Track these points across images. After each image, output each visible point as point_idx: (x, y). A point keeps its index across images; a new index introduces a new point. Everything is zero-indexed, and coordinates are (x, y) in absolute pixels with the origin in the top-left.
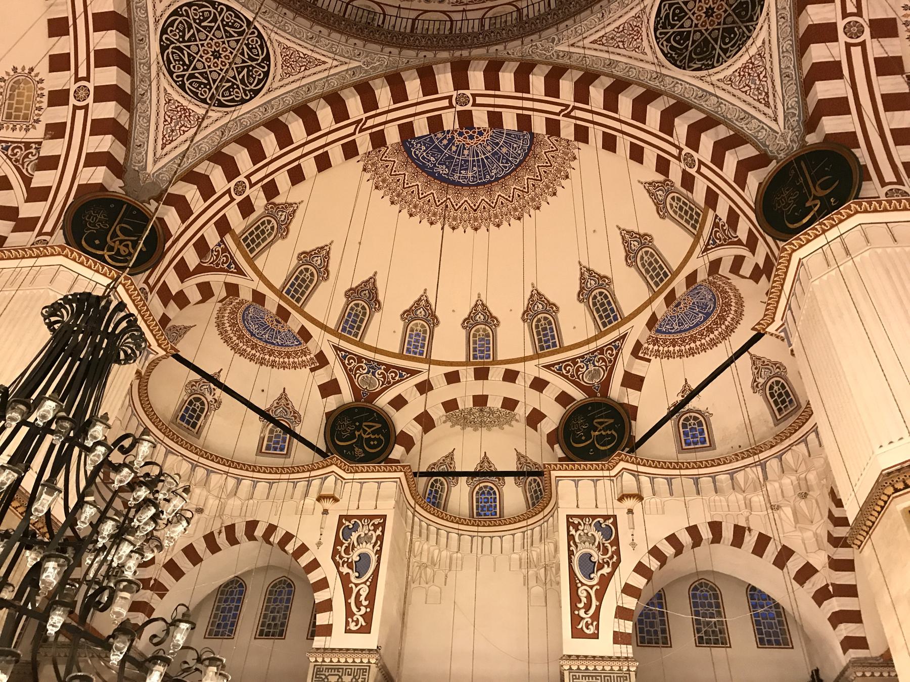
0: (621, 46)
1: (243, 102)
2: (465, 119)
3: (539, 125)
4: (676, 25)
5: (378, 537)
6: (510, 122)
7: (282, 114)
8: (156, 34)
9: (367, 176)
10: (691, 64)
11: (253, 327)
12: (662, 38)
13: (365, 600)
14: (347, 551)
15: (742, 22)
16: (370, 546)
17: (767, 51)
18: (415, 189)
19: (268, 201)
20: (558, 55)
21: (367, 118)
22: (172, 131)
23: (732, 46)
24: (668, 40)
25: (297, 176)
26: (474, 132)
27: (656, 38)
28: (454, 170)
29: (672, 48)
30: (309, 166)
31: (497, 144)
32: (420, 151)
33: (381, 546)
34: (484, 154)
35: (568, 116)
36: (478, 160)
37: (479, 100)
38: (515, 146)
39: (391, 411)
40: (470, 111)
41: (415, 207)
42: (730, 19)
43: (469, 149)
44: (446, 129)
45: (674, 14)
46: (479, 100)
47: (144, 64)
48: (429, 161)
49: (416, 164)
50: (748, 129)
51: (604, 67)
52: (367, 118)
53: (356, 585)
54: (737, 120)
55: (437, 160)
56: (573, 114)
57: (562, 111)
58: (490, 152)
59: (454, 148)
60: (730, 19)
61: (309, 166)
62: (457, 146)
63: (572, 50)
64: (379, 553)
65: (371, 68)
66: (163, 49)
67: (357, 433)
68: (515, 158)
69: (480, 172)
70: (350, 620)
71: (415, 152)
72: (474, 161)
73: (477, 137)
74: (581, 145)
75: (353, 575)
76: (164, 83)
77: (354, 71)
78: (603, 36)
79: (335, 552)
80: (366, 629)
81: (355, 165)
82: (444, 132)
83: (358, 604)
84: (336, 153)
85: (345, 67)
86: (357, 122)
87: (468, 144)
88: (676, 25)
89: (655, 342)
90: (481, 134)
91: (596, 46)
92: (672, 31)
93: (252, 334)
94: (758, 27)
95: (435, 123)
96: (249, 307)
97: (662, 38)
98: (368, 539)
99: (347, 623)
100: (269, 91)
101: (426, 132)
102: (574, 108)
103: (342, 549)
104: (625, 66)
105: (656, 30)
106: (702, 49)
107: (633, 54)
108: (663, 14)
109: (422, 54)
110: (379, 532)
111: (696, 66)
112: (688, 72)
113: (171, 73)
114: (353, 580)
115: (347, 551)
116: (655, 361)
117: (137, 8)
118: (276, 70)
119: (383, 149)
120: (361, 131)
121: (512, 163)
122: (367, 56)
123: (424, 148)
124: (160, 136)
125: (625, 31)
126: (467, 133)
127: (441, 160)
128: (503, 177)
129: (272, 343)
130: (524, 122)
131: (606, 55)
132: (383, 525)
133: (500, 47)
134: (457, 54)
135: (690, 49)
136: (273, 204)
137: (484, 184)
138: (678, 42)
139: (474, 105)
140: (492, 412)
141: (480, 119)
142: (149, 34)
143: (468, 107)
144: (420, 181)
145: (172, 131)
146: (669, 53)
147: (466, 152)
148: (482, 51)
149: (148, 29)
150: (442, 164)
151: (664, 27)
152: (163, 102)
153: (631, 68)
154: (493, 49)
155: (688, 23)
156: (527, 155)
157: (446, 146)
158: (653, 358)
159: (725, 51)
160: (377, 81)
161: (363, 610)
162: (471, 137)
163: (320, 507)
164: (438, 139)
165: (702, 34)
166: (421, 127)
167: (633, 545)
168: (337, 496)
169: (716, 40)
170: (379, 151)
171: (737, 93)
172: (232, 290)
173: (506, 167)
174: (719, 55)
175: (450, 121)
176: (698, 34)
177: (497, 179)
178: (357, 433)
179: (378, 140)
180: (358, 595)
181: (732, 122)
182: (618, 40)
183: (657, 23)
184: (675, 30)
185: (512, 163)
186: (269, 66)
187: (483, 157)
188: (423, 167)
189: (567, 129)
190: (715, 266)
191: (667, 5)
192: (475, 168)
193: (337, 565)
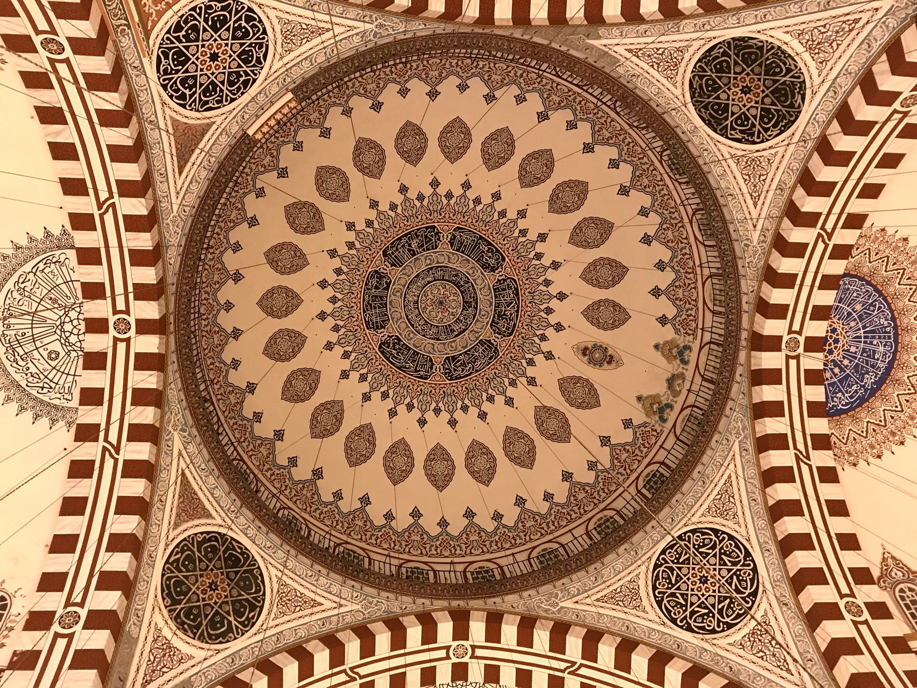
0: (764, 177)
1: (755, 569)
2: (814, 344)
3: (836, 267)
4: (753, 123)
6: (827, 298)
7: (775, 535)
8: (675, 630)
9: (862, 463)
10: (796, 105)
12: (763, 136)
15: (762, 56)
17: (797, 27)
19: (873, 583)
20: (763, 242)
22: (774, 655)
23: (785, 64)
24: (766, 130)
25: (849, 542)
26: (831, 337)
27: (762, 142)
28: (873, 366)
29: (775, 126)
30: (838, 525)
31: (849, 314)
32: (841, 400)
34: (859, 329)
35: (830, 236)
36: (865, 337)
38: (855, 295)
40: (806, 338)
42: (757, 70)
43: (850, 346)
44: (822, 367)
45: (742, 125)
46: (796, 327)
47: (701, 654)
48: (856, 391)
49: (857, 406)
50: (882, 38)
51: (783, 196)
52: (795, 448)
54: (869, 52)
55: (857, 383)
56: (829, 231)
57: (823, 241)
58: (857, 323)
59: (846, 362)
60: (757, 70)
61: (838, 525)
62: (844, 358)
63: (759, 227)
65: (743, 432)
66: (689, 629)
68: (870, 296)
69: (880, 338)
71: (842, 405)
72: (865, 342)
73: (838, 335)
74: (867, 224)
76: (723, 642)
77: (743, 449)
78: (751, 195)
81: (846, 474)
82: (825, 369)
84: (828, 491)
85: (738, 457)
86: (798, 459)
87: (844, 345)
88: (753, 123)
90: (834, 331)
91: (760, 203)
92: (758, 126)
94: (770, 40)
95: (813, 377)
97: (763, 136)
100: (748, 540)
101: (821, 389)
102: (823, 228)
104: (786, 174)
105: (754, 143)
106: (783, 95)
107: (774, 166)
108: (739, 136)
109: (738, 378)
111: (799, 100)
112: (804, 109)
113: (713, 631)
117: (649, 637)
118: (728, 526)
119: (833, 439)
120: (808, 458)
121: (876, 300)
122: (731, 433)
123: (839, 395)
124: (778, 670)
125: (750, 173)
126: (830, 345)
127: (858, 379)
128: (892, 311)
130: (829, 282)
131: (771, 194)
133: (744, 299)
134: (744, 343)
135: (780, 107)
136: (879, 578)
137: (896, 335)
138: (770, 120)
141: (818, 329)
142: (675, 637)
143: (802, 340)
144: (879, 405)
145: (774, 655)
146: (780, 129)
147: (853, 349)
148: (745, 318)
149: (670, 635)
150: (863, 378)
151: (752, 135)
152: (741, 652)
153: (789, 168)
154: (745, 307)
155: (753, 111)
156: (869, 283)
157: (842, 370)
159: (789, 70)
160: (757, 429)
162: (836, 341)
164: (831, 378)
165: (767, 96)
166: (816, 393)
169: (775, 82)
170: (835, 443)
171: (837, 54)
173: (880, 308)
174: (792, 77)
175: (814, 361)
176: (765, 100)
177: (893, 319)
179: (822, 442)
181: (870, 57)
182: (757, 181)
183: (748, 142)
184: (757, 123)
185: (876, 300)
186: (723, 532)
187: (862, 331)
188: (862, 401)
191: (732, 132)
192: (875, 343)
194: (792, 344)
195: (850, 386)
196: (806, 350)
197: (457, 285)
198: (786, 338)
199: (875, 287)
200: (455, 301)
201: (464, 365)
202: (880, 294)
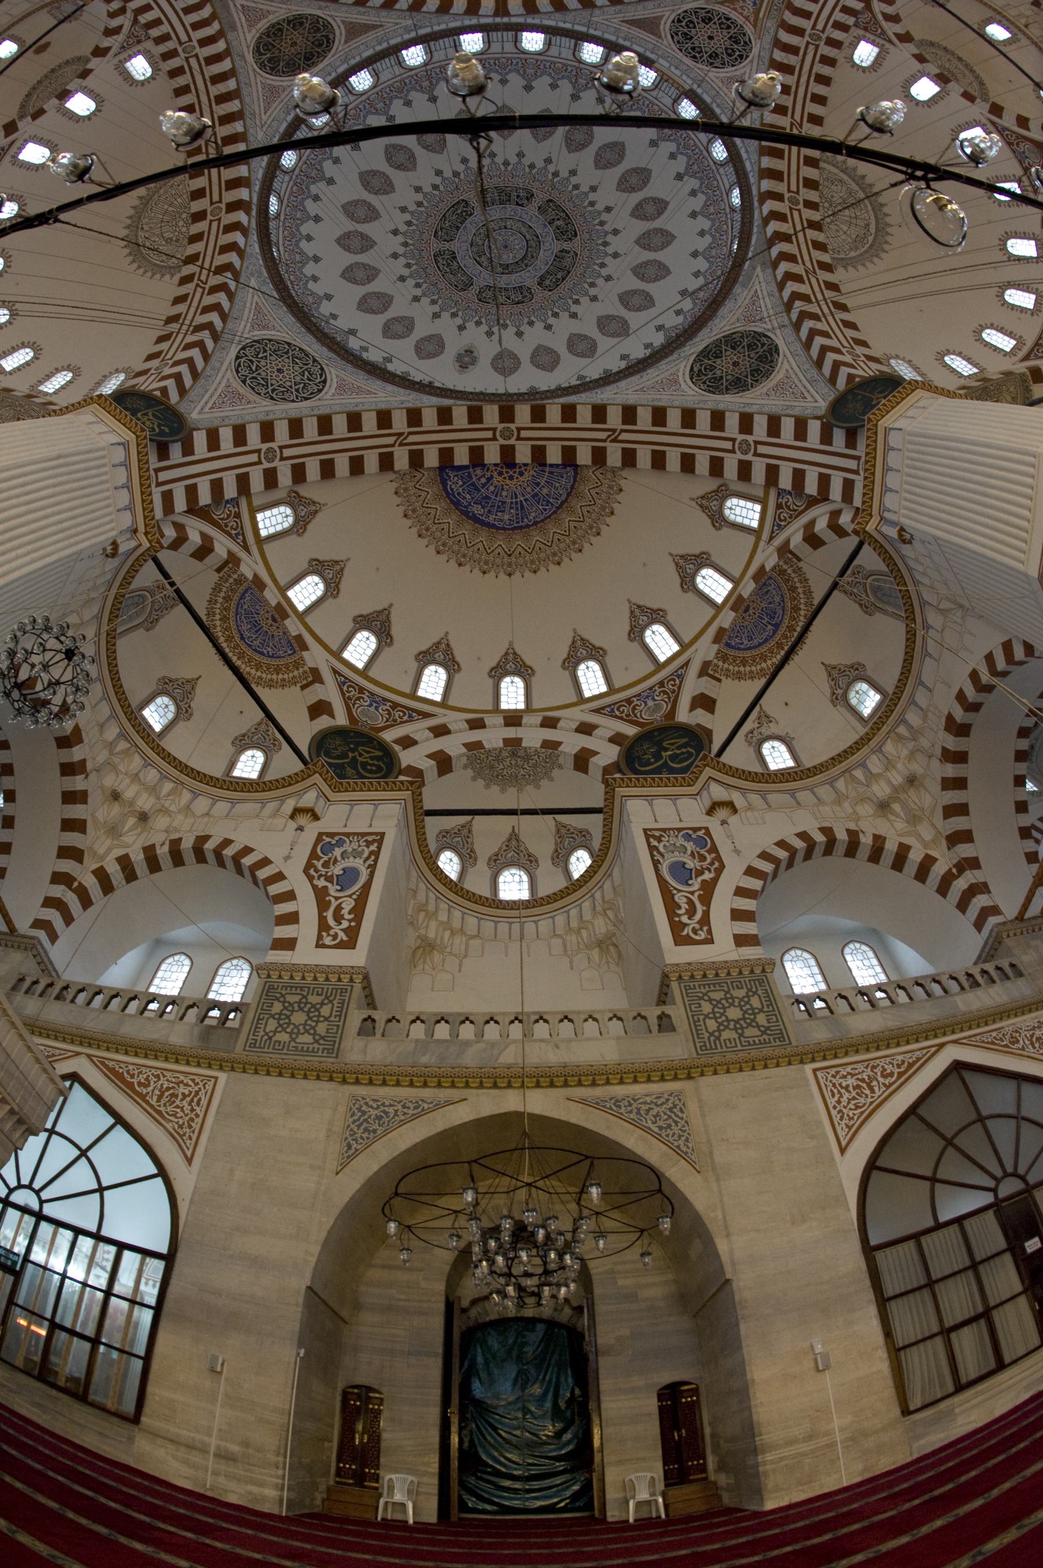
2: (507, 453)
3: (584, 456)
5: (371, 853)
6: (554, 456)
11: (245, 627)
13: (350, 913)
14: (326, 865)
16: (361, 861)
18: (446, 526)
21: (410, 433)
28: (489, 512)
32: (455, 483)
33: (376, 861)
35: (615, 440)
37: (524, 434)
39: (397, 748)
41: (444, 545)
46: (524, 434)
53: (337, 898)
59: (492, 488)
64: (373, 868)
66: (237, 357)
67: (350, 755)
70: (324, 934)
75: (333, 890)
79: (308, 866)
80: (350, 943)
83: (338, 917)
89: (724, 658)
90: (521, 474)
93: (242, 638)
95: (477, 454)
96: (246, 591)
98: (356, 854)
99: (320, 937)
101: (466, 462)
103: (319, 864)
110: (373, 847)
113: (237, 372)
114: (332, 892)
115: (326, 865)
116: (727, 682)
119: (419, 475)
120: (401, 445)
129: (262, 654)
130: (569, 454)
132: (380, 842)
139: (519, 438)
140: (527, 758)
141: (523, 454)
143: (512, 442)
147: (504, 493)
156: (569, 495)
157: (484, 485)
158: (723, 678)
161: (345, 924)
162: (511, 478)
163: (292, 825)
166: (461, 457)
167: (737, 852)
168: (318, 811)
172: (233, 560)
175: (492, 455)
178: (350, 755)
179: (416, 459)
180: (339, 908)
188: (456, 504)
189: (614, 457)
190: (784, 550)
193: (311, 878)
194: (507, 434)
195: (469, 493)
196: (502, 447)
197: (524, 258)
198: (512, 426)
199: (566, 500)
200: (508, 258)
201: (449, 265)
202: (558, 508)
